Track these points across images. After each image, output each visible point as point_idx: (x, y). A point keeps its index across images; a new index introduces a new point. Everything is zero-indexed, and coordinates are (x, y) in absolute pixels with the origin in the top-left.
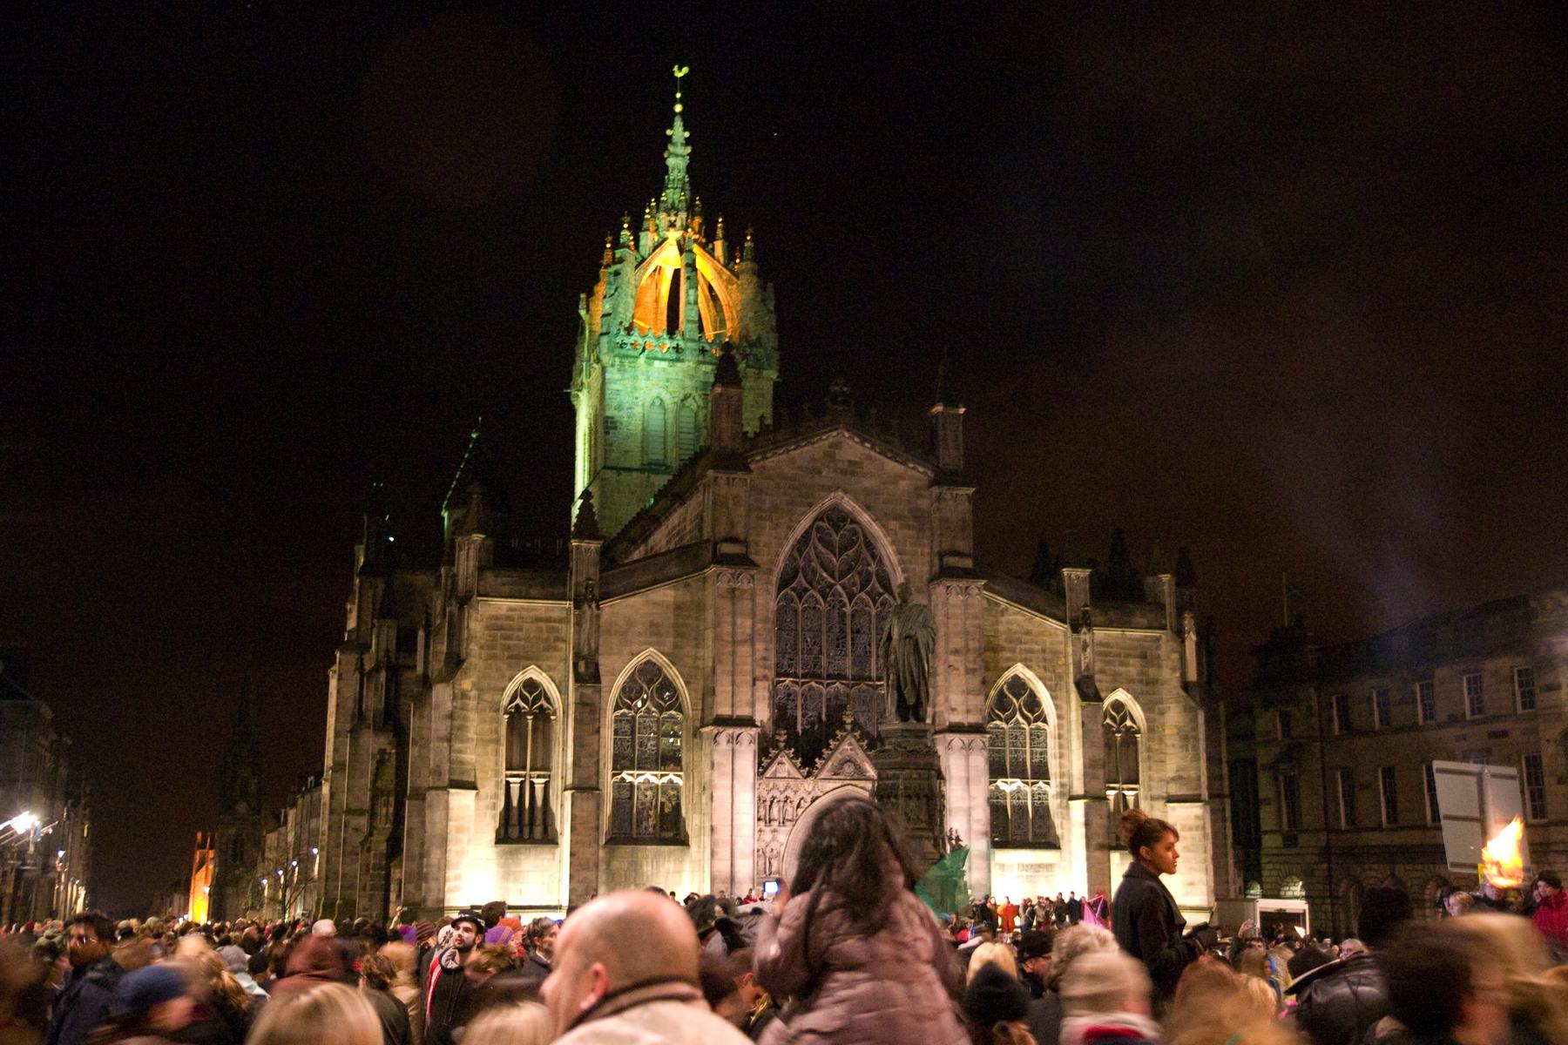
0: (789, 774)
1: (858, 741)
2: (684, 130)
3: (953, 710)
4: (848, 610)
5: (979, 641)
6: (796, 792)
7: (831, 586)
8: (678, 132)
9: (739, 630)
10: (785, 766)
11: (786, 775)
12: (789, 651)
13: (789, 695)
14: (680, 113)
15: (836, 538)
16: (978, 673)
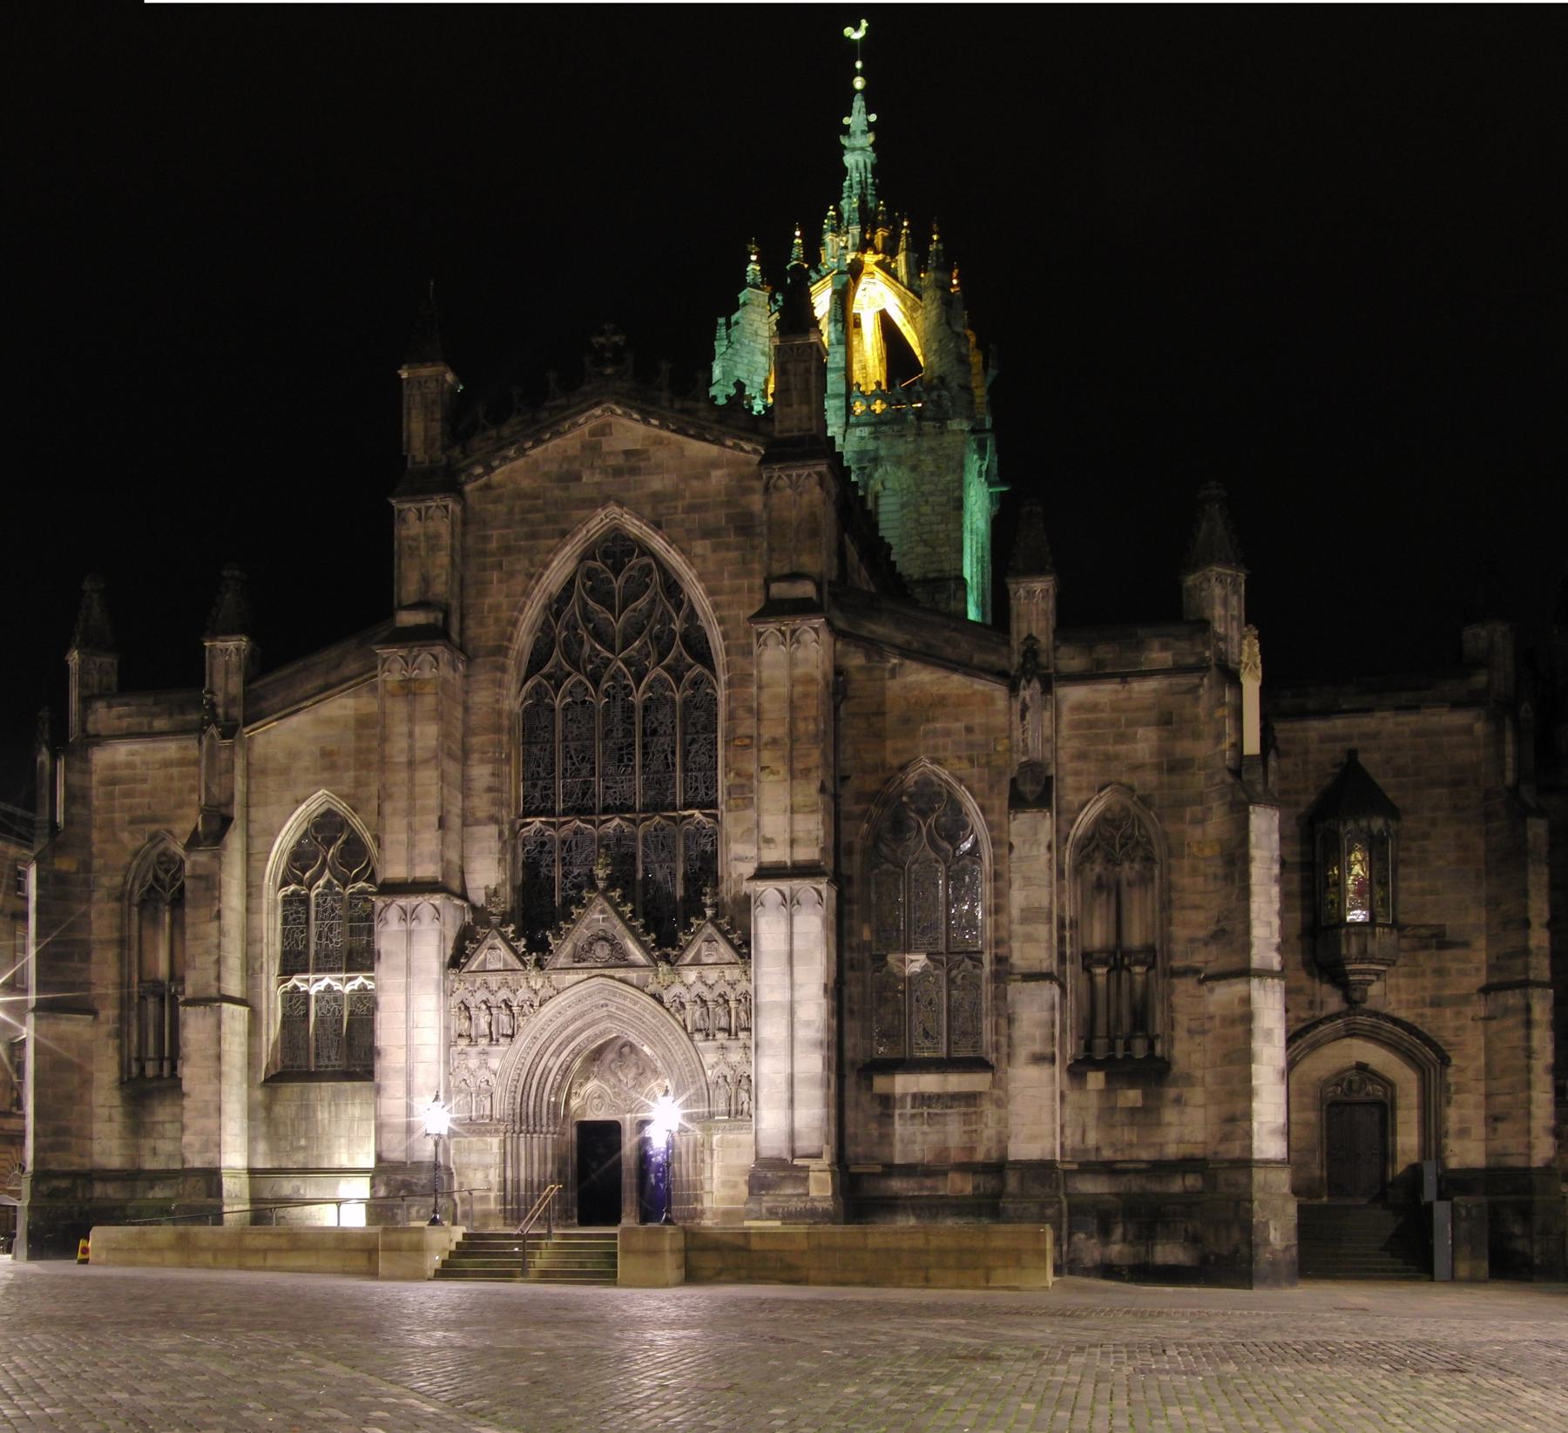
0: (505, 963)
1: (615, 906)
2: (868, 113)
3: (768, 841)
4: (638, 698)
5: (815, 719)
6: (515, 992)
7: (607, 663)
8: (858, 119)
9: (419, 744)
10: (495, 954)
11: (500, 966)
12: (543, 775)
13: (543, 844)
14: (861, 91)
15: (618, 583)
16: (814, 774)
